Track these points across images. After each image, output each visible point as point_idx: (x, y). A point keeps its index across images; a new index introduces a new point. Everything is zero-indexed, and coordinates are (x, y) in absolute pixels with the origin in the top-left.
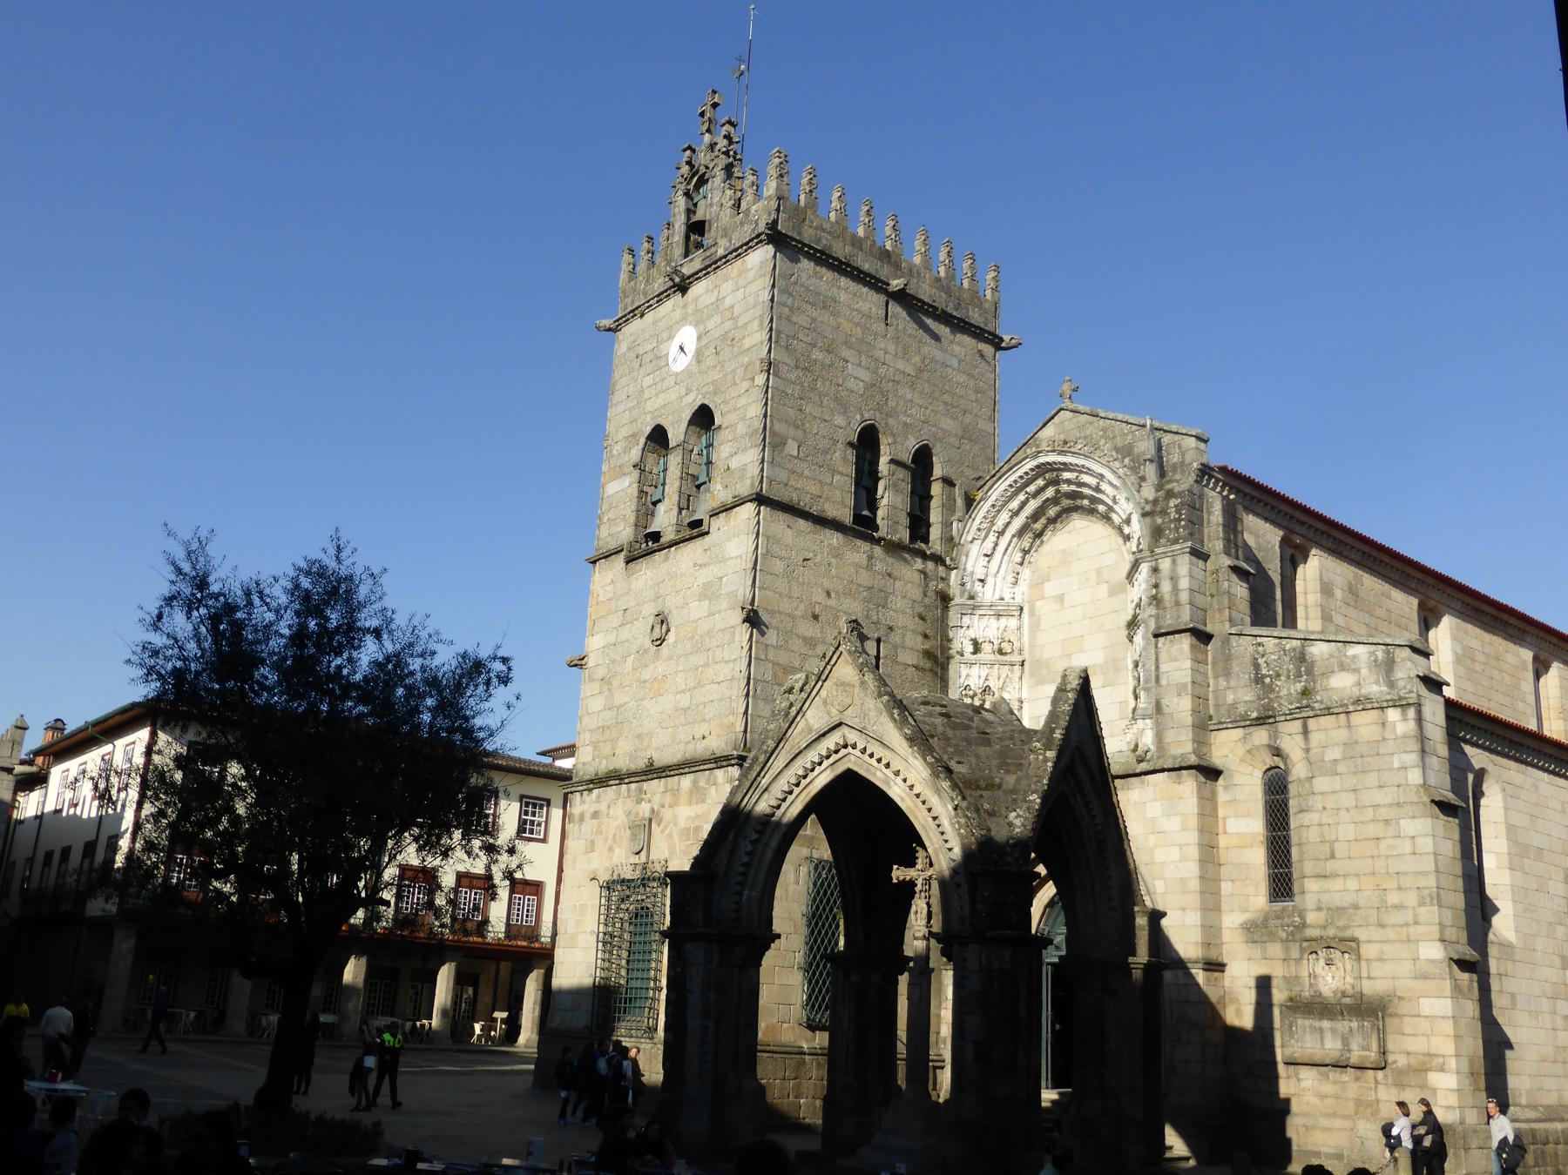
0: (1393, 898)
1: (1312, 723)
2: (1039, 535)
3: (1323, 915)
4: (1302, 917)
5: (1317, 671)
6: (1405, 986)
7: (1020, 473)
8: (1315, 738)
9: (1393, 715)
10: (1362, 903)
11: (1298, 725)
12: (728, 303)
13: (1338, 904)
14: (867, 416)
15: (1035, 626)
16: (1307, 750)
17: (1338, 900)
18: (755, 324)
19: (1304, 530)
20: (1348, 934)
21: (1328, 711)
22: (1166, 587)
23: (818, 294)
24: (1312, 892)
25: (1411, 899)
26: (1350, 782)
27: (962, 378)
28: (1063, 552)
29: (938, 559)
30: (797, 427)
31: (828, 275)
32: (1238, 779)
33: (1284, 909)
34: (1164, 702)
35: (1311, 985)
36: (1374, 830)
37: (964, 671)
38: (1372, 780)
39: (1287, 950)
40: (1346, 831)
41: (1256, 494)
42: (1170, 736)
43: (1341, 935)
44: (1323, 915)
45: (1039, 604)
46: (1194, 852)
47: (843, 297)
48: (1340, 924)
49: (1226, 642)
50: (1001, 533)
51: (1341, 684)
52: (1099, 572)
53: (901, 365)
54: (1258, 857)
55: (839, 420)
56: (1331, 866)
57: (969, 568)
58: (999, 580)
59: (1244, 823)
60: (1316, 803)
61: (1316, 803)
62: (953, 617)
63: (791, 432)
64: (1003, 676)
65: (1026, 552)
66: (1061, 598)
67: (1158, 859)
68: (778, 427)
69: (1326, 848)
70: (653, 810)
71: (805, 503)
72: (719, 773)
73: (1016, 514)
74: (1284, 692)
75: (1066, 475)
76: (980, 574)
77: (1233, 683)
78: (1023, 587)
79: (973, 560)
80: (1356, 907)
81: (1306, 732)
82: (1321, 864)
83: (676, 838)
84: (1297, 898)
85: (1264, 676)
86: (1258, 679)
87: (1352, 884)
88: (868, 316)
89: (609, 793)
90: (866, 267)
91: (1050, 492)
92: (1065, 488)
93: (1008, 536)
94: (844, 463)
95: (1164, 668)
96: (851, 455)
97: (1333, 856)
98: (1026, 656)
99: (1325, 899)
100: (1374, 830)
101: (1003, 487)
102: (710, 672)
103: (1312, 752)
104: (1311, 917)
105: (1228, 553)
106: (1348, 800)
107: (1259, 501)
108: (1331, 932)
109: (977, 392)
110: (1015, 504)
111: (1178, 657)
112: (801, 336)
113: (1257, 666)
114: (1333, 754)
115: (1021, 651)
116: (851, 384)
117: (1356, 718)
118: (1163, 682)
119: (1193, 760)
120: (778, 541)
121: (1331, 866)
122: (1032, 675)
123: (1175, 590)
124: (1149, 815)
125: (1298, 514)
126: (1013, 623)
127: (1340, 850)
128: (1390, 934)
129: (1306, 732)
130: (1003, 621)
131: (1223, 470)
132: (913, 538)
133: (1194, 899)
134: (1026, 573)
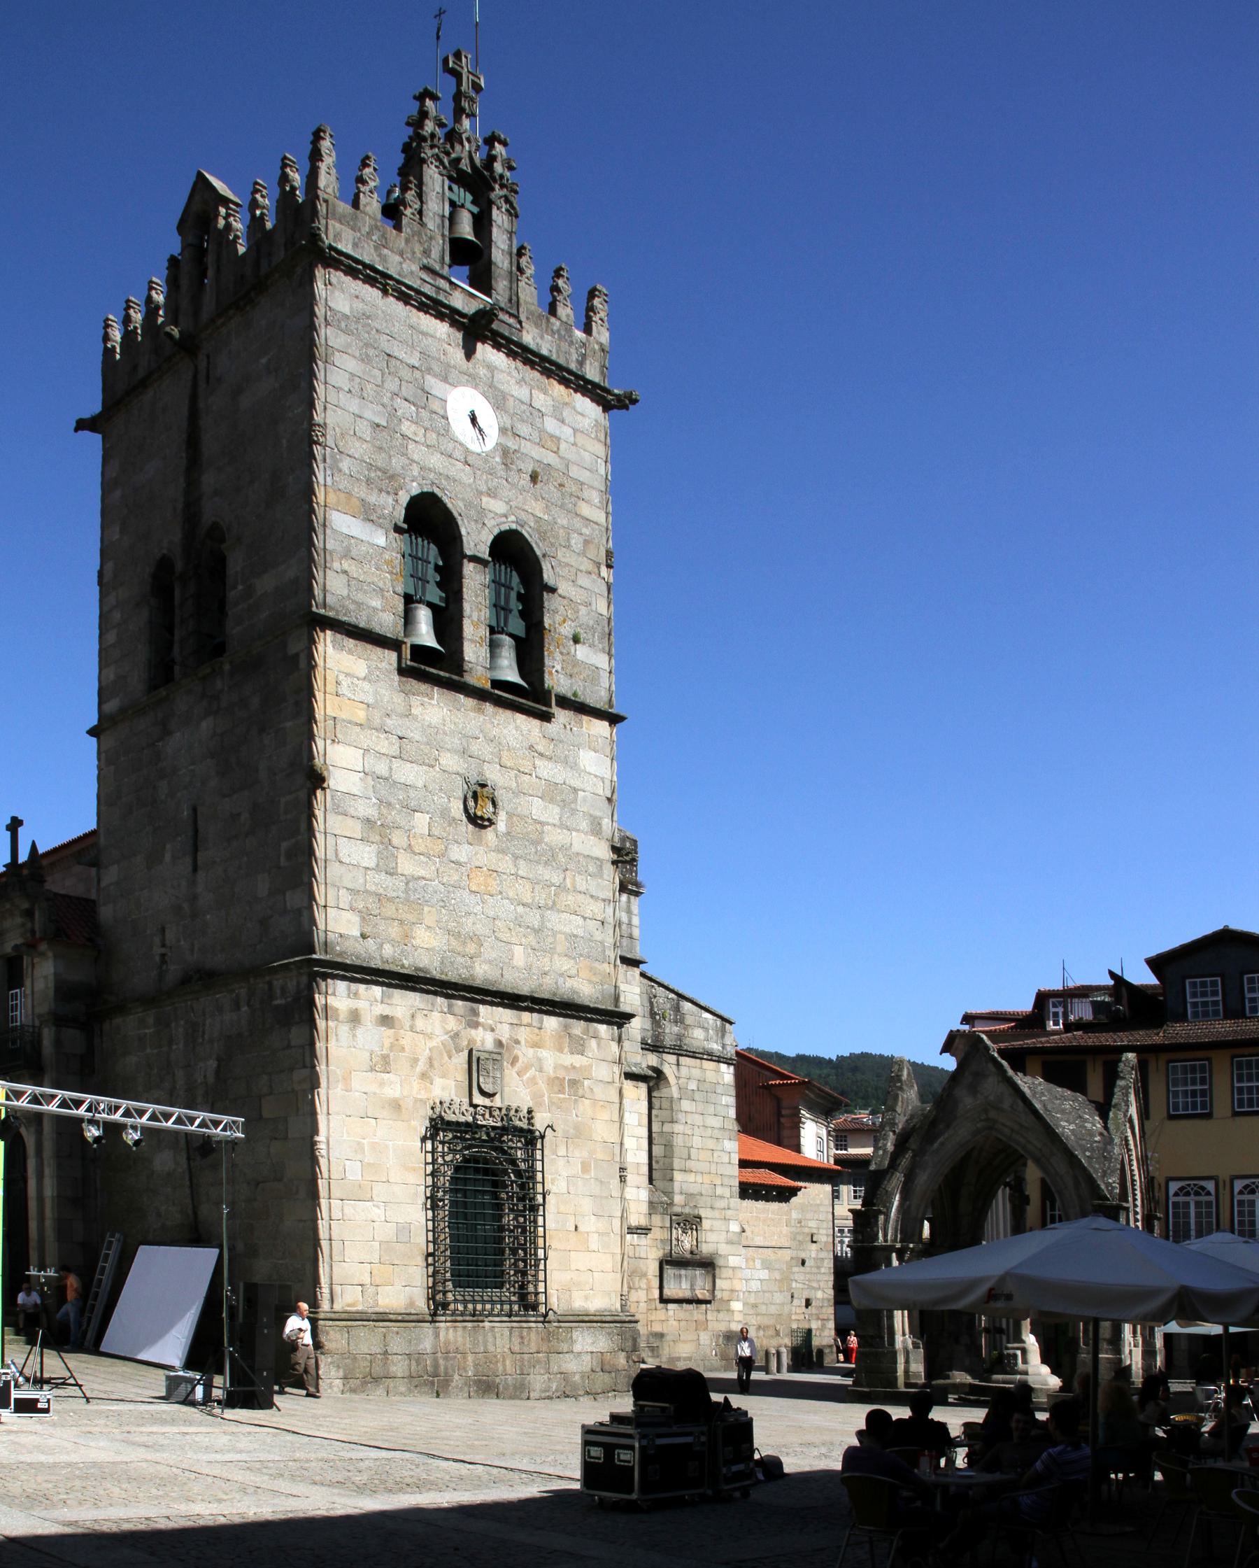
0: (719, 1191)
4: (672, 1199)
6: (723, 1249)
9: (723, 1067)
11: (674, 1057)
13: (691, 1191)
16: (678, 1078)
17: (694, 1189)
21: (693, 1055)
25: (727, 1193)
26: (701, 1107)
36: (711, 1144)
38: (711, 1109)
39: (663, 1220)
40: (697, 1142)
56: (690, 1164)
60: (681, 1117)
70: (500, 1044)
72: (603, 1029)
81: (678, 1065)
83: (543, 1086)
85: (656, 1014)
87: (699, 1179)
89: (413, 1000)
100: (711, 1144)
102: (570, 899)
104: (678, 1199)
106: (698, 1119)
108: (687, 1210)
113: (651, 1003)
121: (690, 1164)
127: (693, 1152)
128: (716, 1214)
129: (678, 1065)
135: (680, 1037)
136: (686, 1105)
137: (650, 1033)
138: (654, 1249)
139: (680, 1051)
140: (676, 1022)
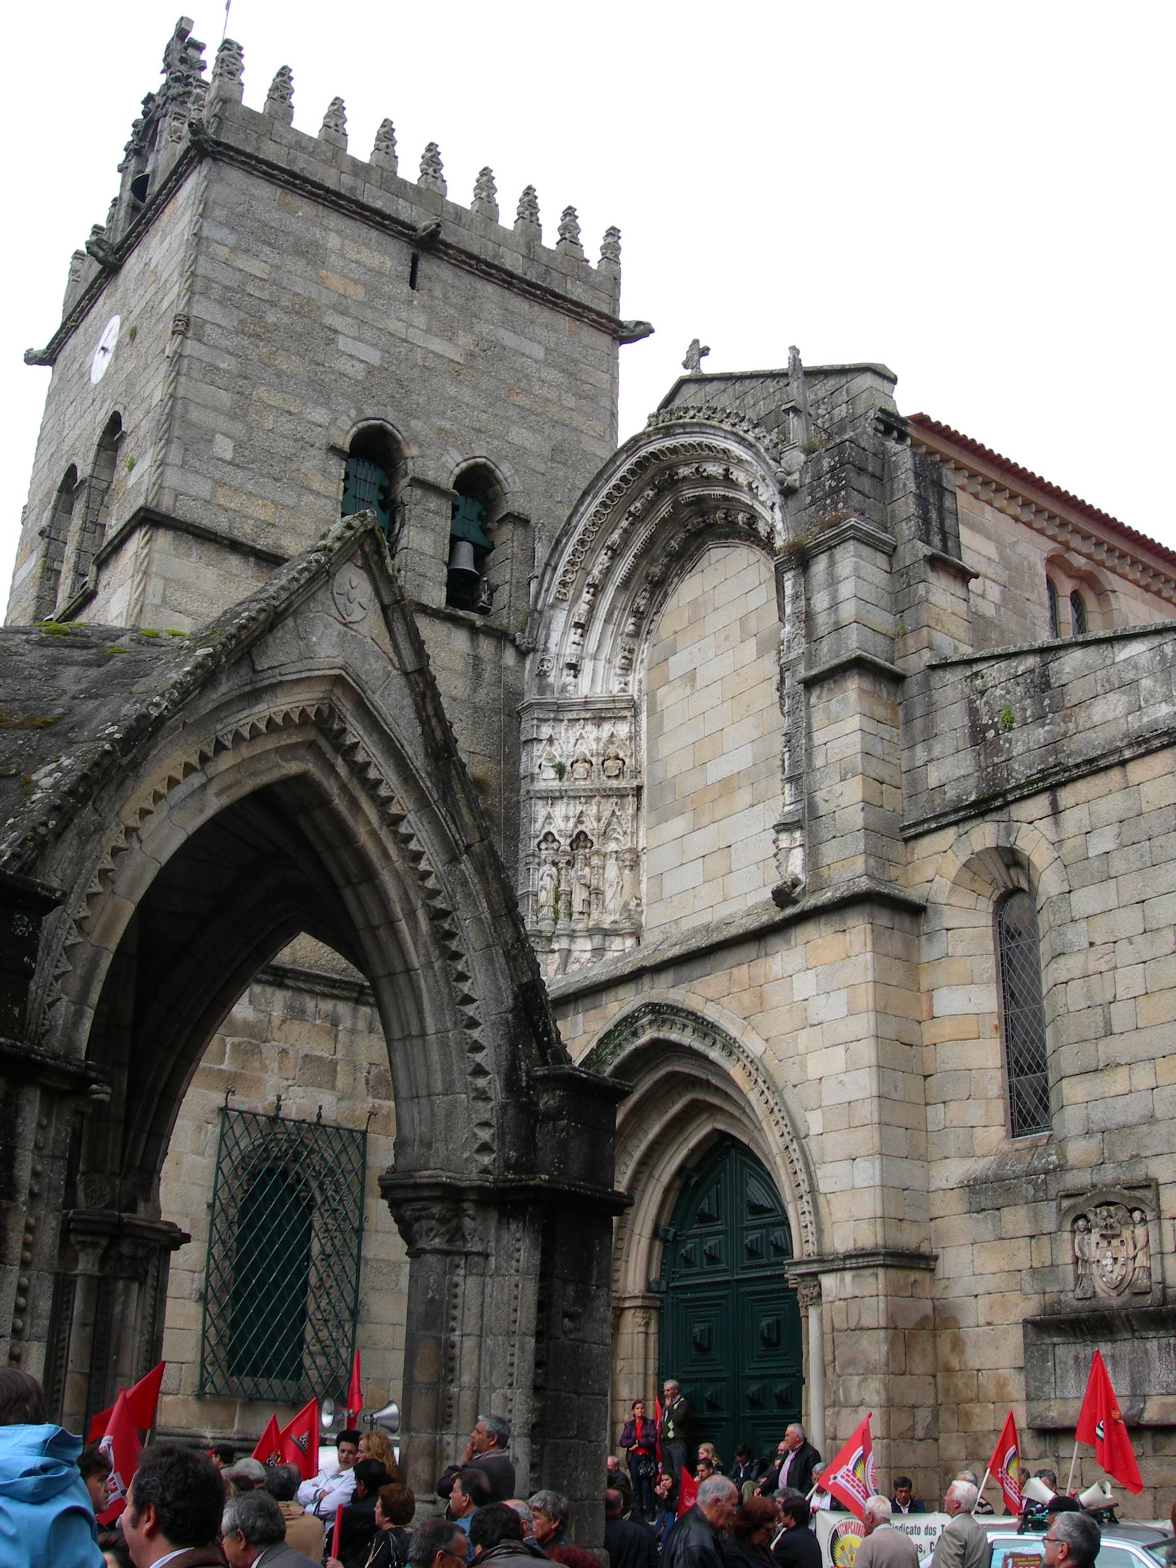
1: (1066, 796)
2: (659, 587)
3: (1094, 1143)
4: (1062, 1154)
5: (1071, 699)
7: (613, 482)
8: (1072, 820)
10: (1159, 1115)
11: (1043, 801)
12: (153, 264)
13: (1121, 1119)
14: (369, 412)
15: (656, 732)
16: (1058, 844)
18: (175, 277)
19: (1088, 547)
20: (1139, 1173)
21: (1093, 767)
22: (821, 601)
23: (287, 234)
24: (1074, 1098)
27: (551, 375)
28: (694, 603)
29: (502, 637)
30: (234, 417)
31: (305, 208)
32: (949, 918)
33: (1034, 1146)
34: (819, 796)
35: (1078, 1278)
37: (541, 810)
39: (1036, 1218)
41: (993, 475)
42: (830, 852)
43: (1125, 1177)
44: (1094, 1143)
45: (660, 693)
46: (867, 1052)
47: (333, 241)
48: (1123, 1156)
49: (926, 686)
50: (597, 589)
51: (1107, 717)
52: (743, 620)
53: (438, 345)
54: (988, 1056)
55: (319, 415)
57: (553, 648)
58: (601, 664)
59: (965, 998)
61: (1077, 936)
62: (528, 728)
63: (223, 423)
64: (606, 814)
65: (639, 615)
66: (690, 677)
67: (813, 1072)
68: (195, 414)
69: (1097, 1016)
71: (244, 532)
73: (616, 553)
74: (1018, 749)
75: (684, 471)
76: (570, 653)
77: (937, 751)
78: (639, 673)
79: (560, 640)
80: (1151, 1119)
81: (1056, 811)
82: (1089, 1046)
84: (1055, 1122)
85: (986, 728)
86: (977, 734)
87: (1143, 1077)
88: (380, 273)
90: (379, 205)
91: (665, 509)
92: (689, 493)
93: (610, 591)
94: (326, 481)
95: (819, 738)
96: (338, 468)
97: (1109, 1032)
98: (644, 779)
99: (1098, 1114)
101: (592, 510)
103: (1067, 847)
104: (1078, 1150)
105: (928, 542)
106: (1129, 921)
107: (1000, 489)
108: (1109, 1173)
109: (580, 396)
110: (616, 536)
111: (845, 723)
112: (250, 289)
114: (1104, 841)
115: (637, 773)
116: (344, 365)
117: (1136, 771)
118: (819, 762)
119: (864, 884)
120: (184, 586)
122: (652, 808)
123: (834, 606)
124: (798, 997)
125: (1073, 518)
126: (623, 729)
127: (1121, 1016)
129: (1056, 811)
130: (607, 728)
131: (921, 421)
132: (453, 599)
133: (867, 1139)
134: (645, 651)
135: (1053, 745)
136: (1086, 900)
137: (972, 781)
138: (1015, 1297)
139: (1052, 780)
140: (1040, 718)
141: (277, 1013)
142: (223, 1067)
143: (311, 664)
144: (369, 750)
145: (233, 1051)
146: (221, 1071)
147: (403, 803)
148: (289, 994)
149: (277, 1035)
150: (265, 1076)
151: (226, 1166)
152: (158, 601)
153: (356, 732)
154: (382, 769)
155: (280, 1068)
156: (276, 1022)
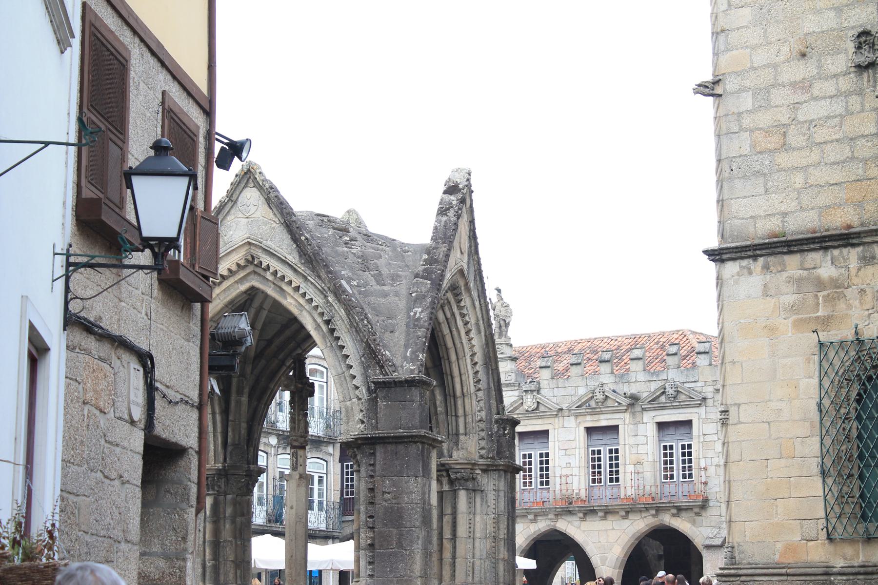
141: (854, 264)
142: (819, 314)
143: (231, 244)
144: (275, 265)
145: (825, 301)
146: (818, 317)
147: (297, 281)
148: (860, 249)
149: (855, 280)
150: (851, 312)
151: (826, 383)
152: (725, 7)
153: (266, 260)
154: (283, 270)
155: (861, 304)
156: (853, 272)
